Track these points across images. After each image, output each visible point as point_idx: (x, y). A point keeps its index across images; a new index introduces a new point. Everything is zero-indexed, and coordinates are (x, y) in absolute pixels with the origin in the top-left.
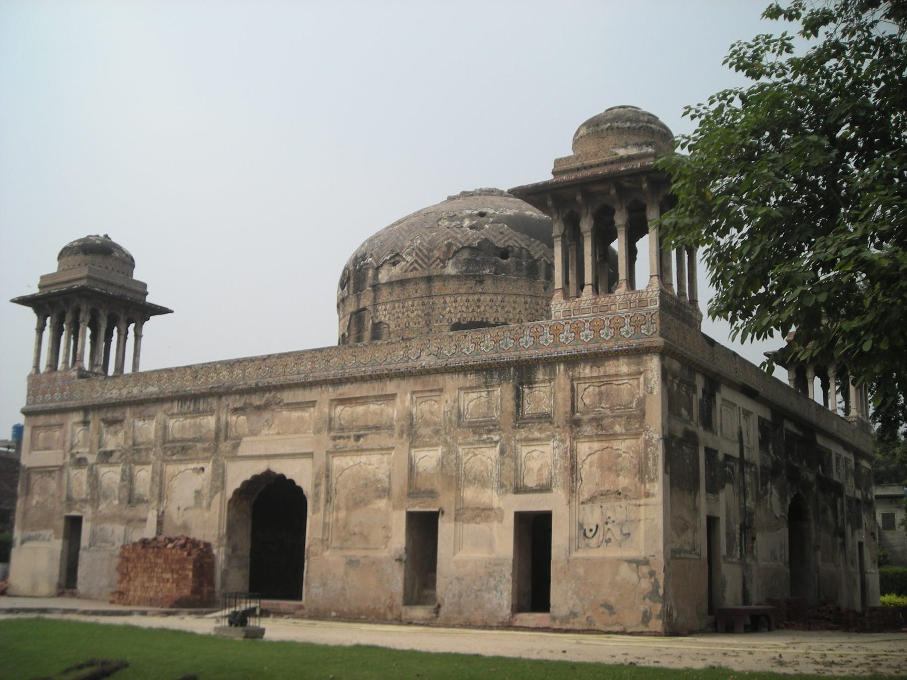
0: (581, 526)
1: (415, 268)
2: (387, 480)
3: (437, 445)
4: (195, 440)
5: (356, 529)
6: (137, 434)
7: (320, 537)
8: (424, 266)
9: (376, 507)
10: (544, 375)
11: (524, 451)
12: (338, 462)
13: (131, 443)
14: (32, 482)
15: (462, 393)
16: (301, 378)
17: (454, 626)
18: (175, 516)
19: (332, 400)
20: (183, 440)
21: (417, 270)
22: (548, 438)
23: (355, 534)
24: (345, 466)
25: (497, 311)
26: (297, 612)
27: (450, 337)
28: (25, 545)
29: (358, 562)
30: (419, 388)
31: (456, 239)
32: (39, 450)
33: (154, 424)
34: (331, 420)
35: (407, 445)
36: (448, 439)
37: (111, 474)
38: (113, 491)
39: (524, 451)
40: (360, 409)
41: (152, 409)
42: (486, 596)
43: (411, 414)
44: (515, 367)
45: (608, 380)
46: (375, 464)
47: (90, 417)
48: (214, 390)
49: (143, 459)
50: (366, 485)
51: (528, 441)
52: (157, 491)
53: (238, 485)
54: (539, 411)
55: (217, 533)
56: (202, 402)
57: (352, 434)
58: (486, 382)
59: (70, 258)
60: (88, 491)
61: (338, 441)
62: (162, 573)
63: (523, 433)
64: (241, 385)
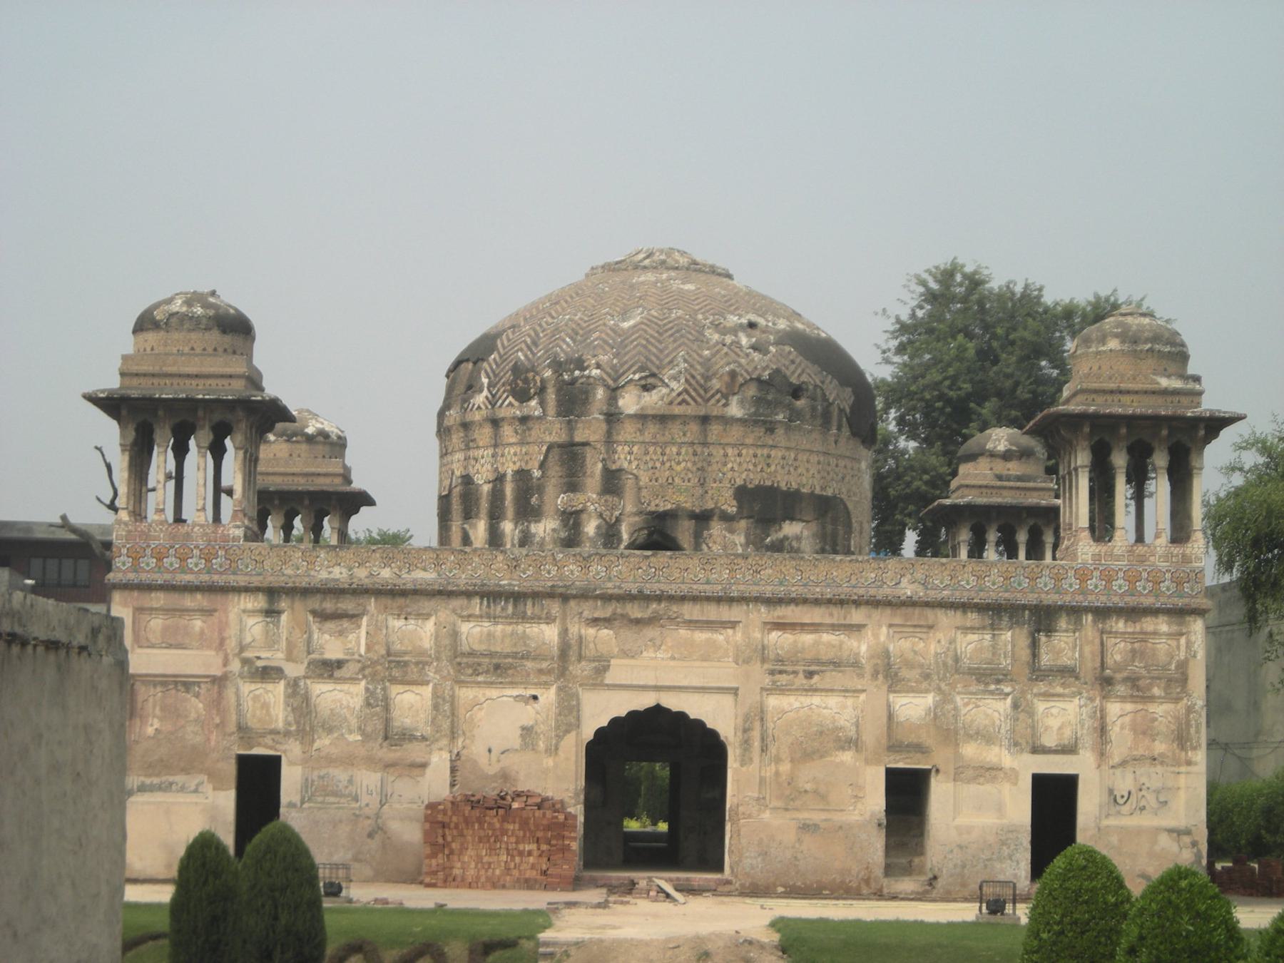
0: (1111, 791)
1: (684, 401)
2: (854, 728)
3: (927, 691)
4: (514, 655)
5: (808, 787)
6: (393, 638)
7: (756, 795)
8: (699, 400)
9: (838, 760)
10: (1068, 623)
11: (1041, 706)
12: (773, 702)
13: (383, 652)
14: (140, 698)
15: (959, 632)
16: (717, 589)
17: (955, 900)
18: (483, 761)
19: (765, 623)
20: (491, 655)
21: (688, 404)
22: (1073, 695)
23: (806, 791)
24: (786, 707)
25: (789, 473)
26: (720, 889)
27: (943, 564)
28: (132, 799)
29: (815, 825)
30: (897, 621)
31: (740, 365)
32: (153, 646)
33: (430, 626)
34: (764, 648)
35: (885, 688)
36: (943, 685)
37: (340, 695)
38: (346, 719)
39: (1041, 706)
40: (807, 638)
41: (426, 605)
42: (998, 866)
43: (887, 654)
44: (1030, 610)
45: (1144, 636)
46: (833, 708)
47: (283, 604)
48: (560, 590)
49: (415, 677)
50: (821, 733)
51: (1047, 696)
52: (446, 725)
53: (604, 722)
54: (1059, 663)
55: (572, 787)
56: (529, 603)
57: (800, 668)
58: (992, 625)
59: (193, 336)
60: (291, 718)
61: (778, 677)
62: (517, 843)
63: (1042, 687)
64: (610, 588)
